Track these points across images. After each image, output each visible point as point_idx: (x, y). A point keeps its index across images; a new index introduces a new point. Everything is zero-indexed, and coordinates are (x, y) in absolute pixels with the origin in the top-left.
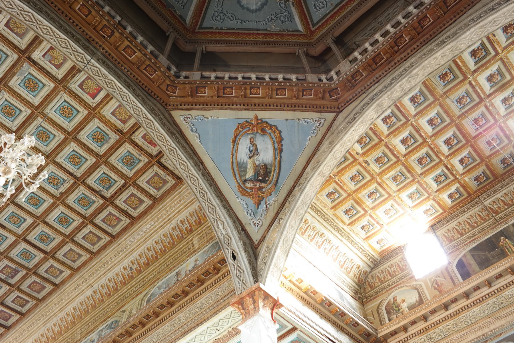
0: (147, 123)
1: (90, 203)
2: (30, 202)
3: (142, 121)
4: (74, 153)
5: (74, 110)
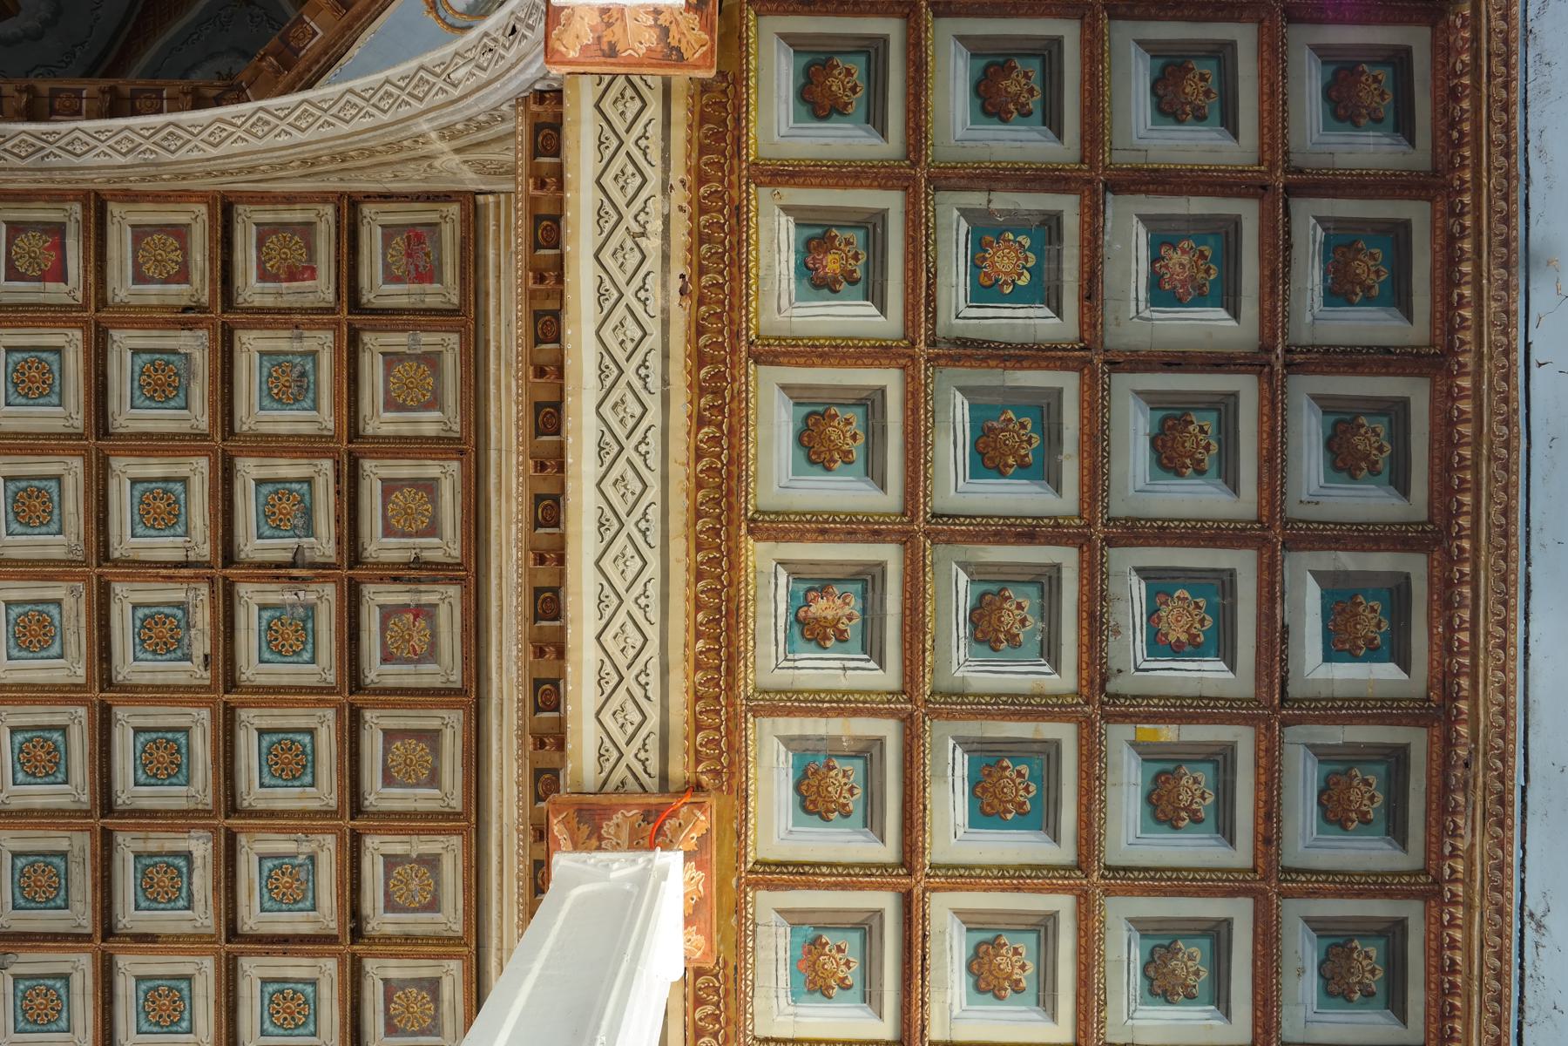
0: (165, 144)
1: (304, 621)
2: (155, 775)
3: (152, 152)
4: (140, 487)
5: (44, 355)
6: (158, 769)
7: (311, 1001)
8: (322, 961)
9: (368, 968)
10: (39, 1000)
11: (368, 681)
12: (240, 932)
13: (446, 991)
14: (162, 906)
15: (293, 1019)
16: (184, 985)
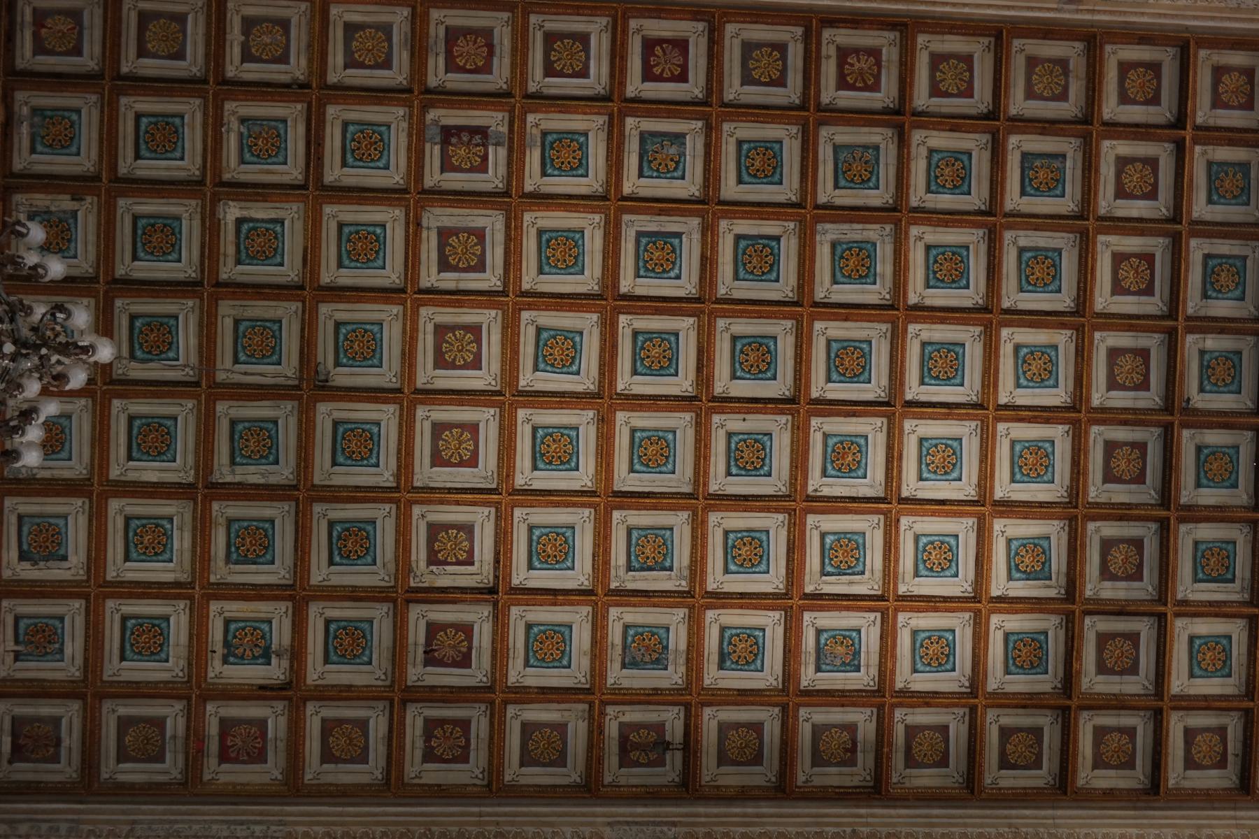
1: (45, 117)
2: (173, 245)
6: (167, 243)
7: (361, 127)
8: (329, 118)
9: (335, 80)
10: (356, 346)
11: (96, 68)
12: (303, 183)
13: (356, 18)
14: (280, 245)
15: (376, 143)
16: (346, 230)
